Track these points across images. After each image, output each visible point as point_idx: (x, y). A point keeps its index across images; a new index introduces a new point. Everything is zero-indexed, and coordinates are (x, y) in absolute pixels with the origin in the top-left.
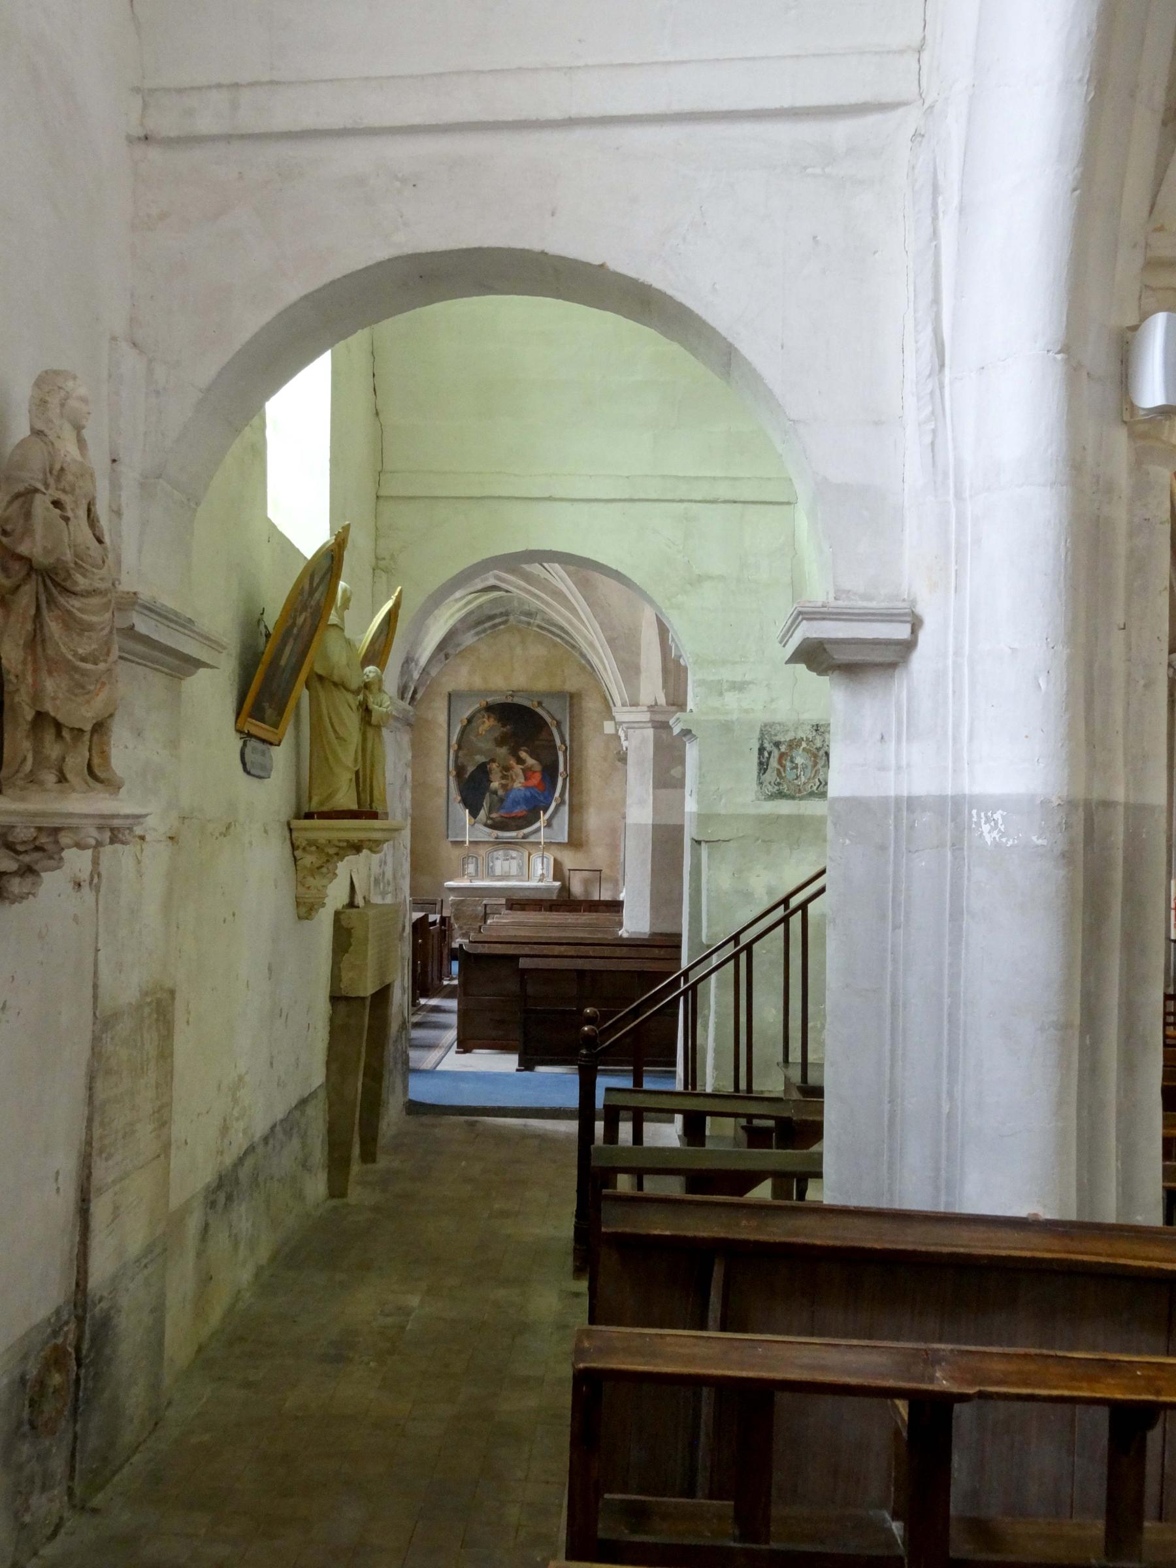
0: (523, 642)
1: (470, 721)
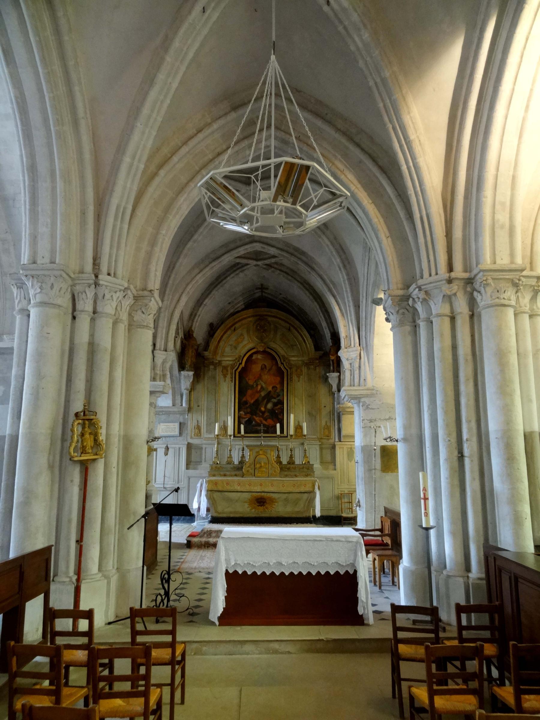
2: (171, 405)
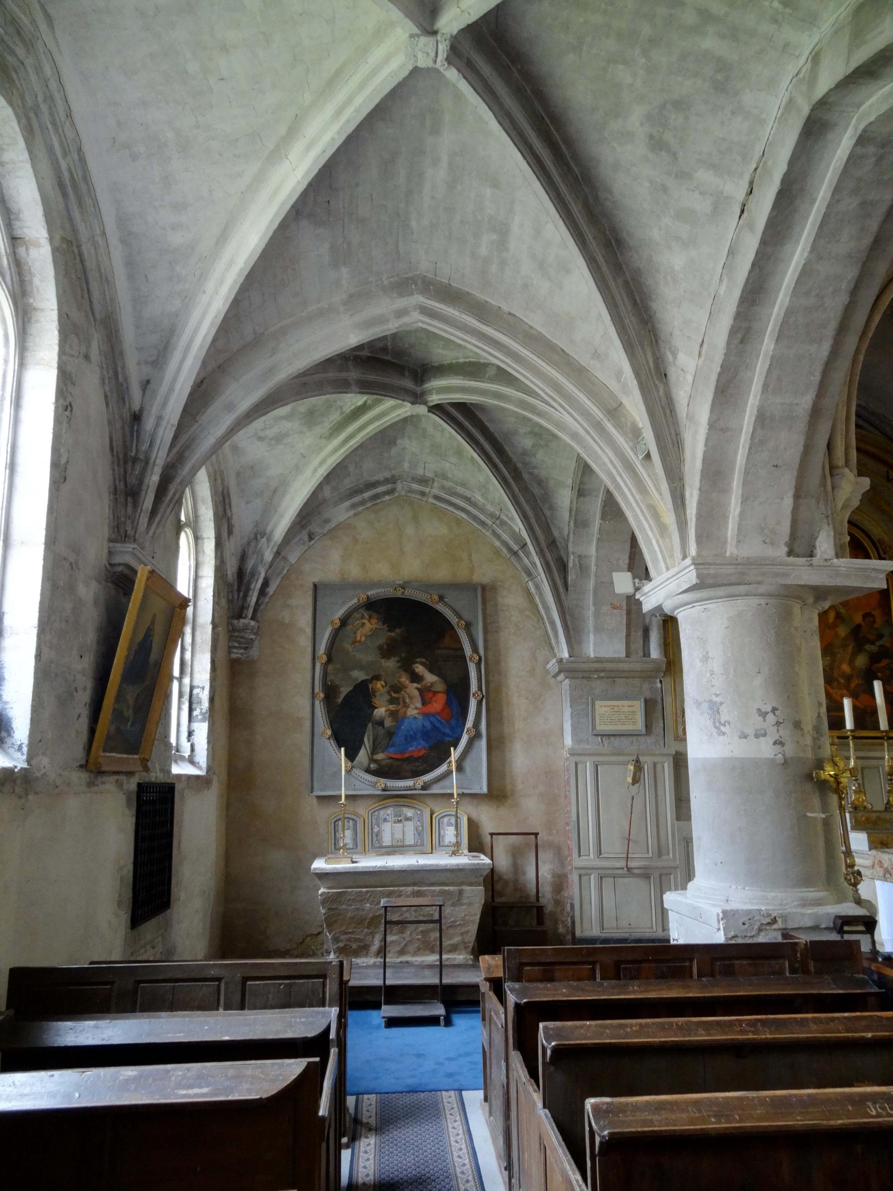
0: (415, 518)
1: (344, 622)
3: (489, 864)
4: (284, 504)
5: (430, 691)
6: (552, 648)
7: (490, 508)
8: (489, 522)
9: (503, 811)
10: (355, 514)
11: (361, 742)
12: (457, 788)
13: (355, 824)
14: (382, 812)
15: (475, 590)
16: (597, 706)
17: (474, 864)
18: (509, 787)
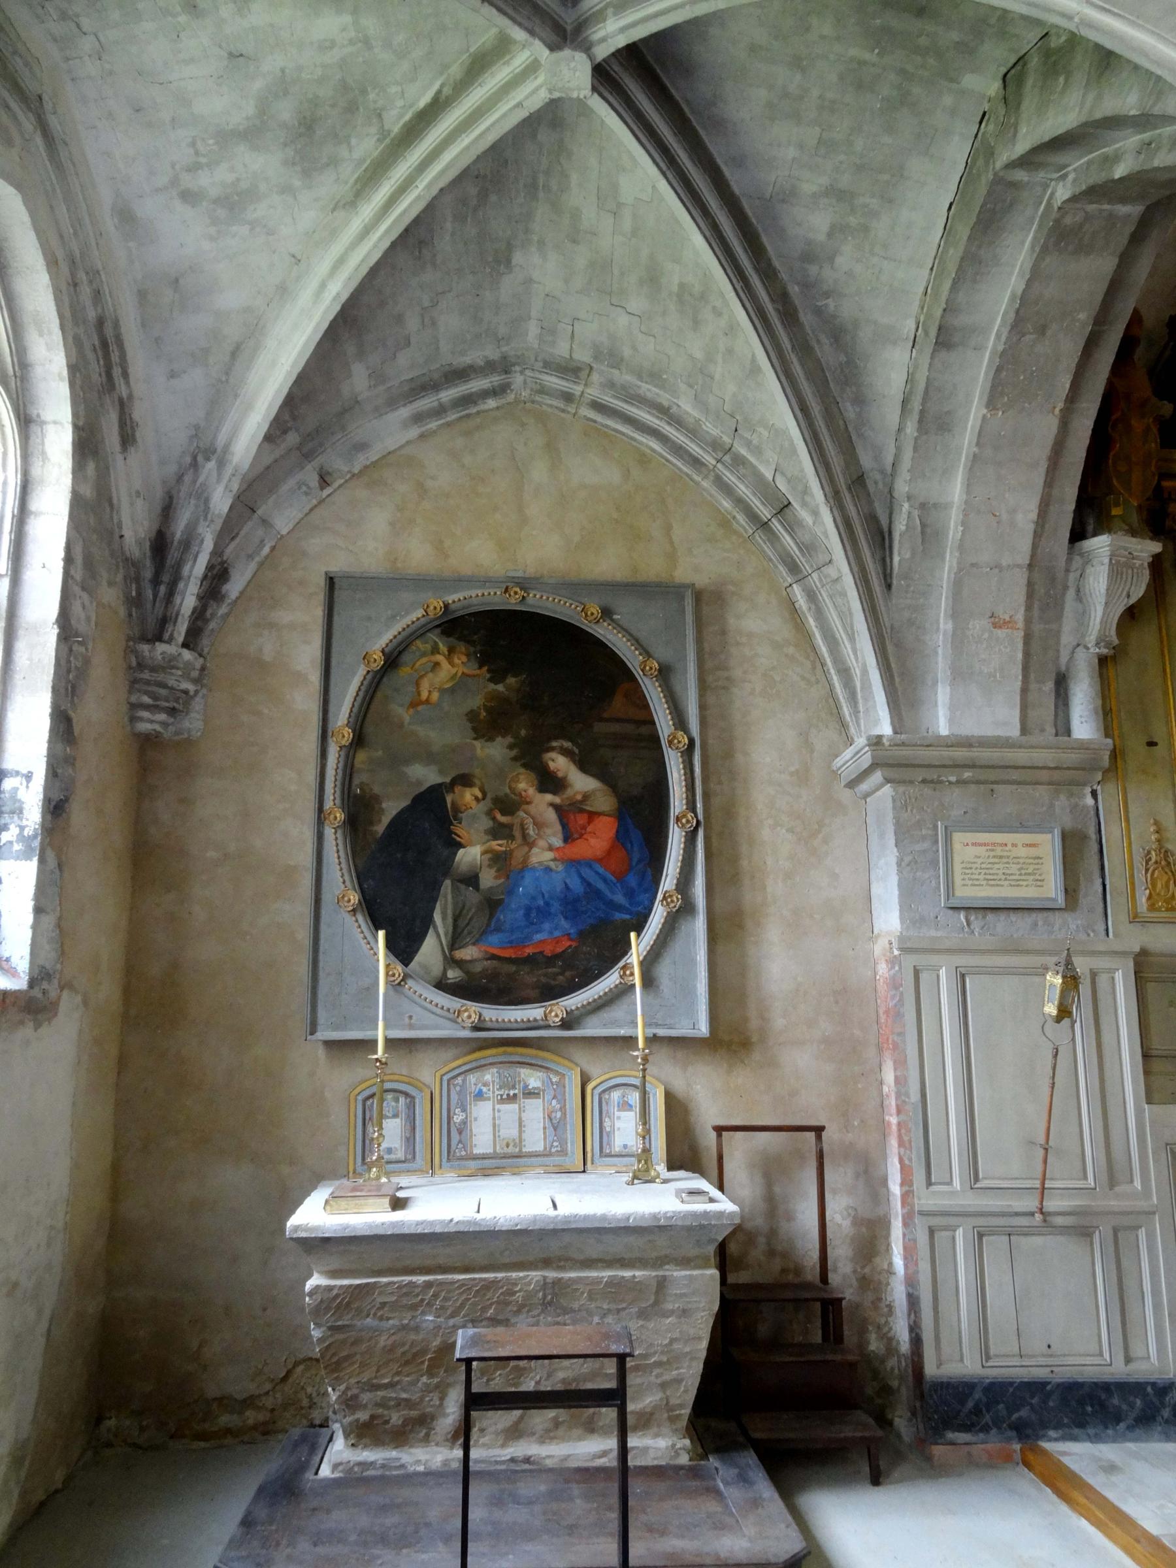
1: (393, 659)
2: (1014, 731)
3: (732, 1214)
4: (253, 378)
5: (582, 811)
6: (844, 725)
7: (711, 429)
8: (709, 460)
9: (742, 1077)
10: (422, 436)
11: (427, 922)
12: (646, 1025)
13: (411, 1106)
14: (472, 1078)
15: (681, 598)
16: (957, 846)
17: (694, 1215)
18: (754, 1024)
